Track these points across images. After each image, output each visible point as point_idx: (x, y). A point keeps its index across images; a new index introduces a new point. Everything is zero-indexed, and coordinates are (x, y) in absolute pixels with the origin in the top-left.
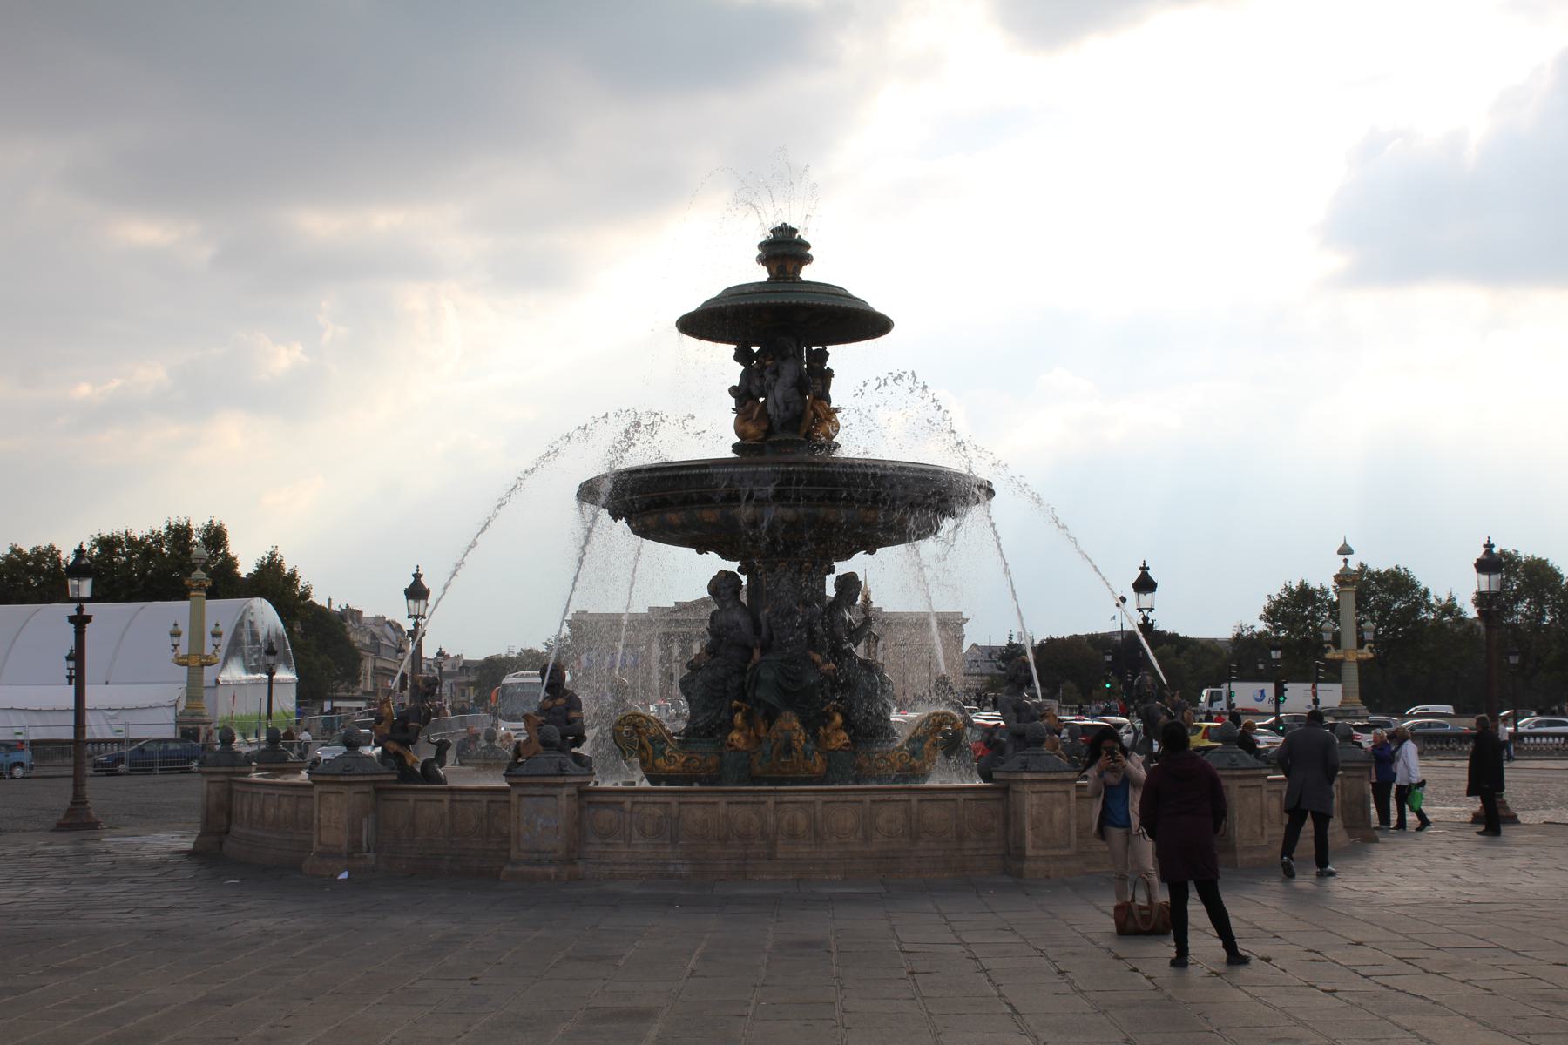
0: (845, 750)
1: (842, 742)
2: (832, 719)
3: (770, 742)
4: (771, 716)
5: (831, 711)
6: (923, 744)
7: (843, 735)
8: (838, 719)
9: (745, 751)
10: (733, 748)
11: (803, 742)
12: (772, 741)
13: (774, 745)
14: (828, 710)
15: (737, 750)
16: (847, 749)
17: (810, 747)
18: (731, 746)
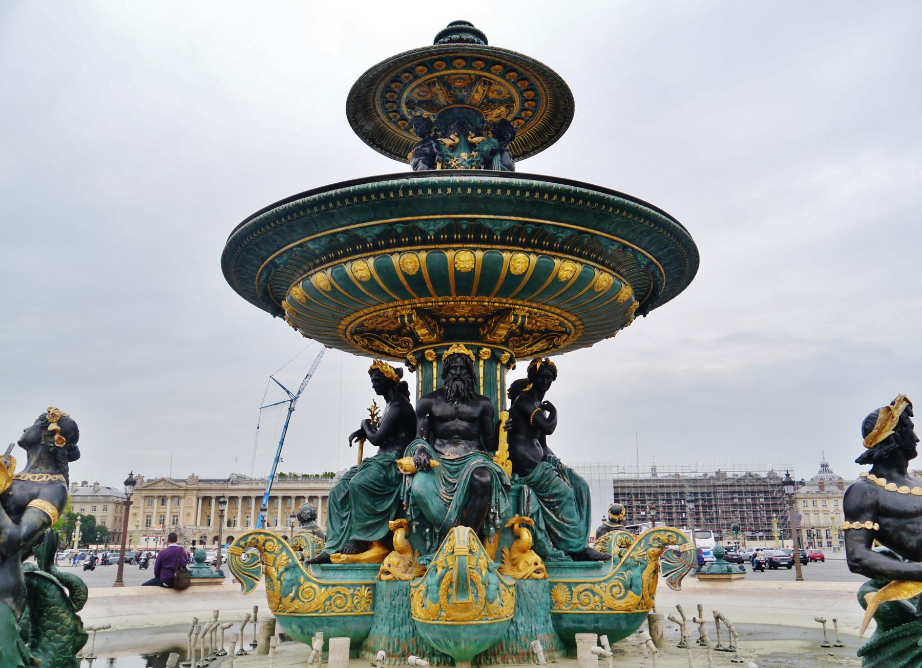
0: (537, 579)
1: (534, 568)
2: (518, 537)
3: (437, 570)
4: (441, 532)
5: (516, 526)
6: (642, 571)
7: (534, 557)
8: (526, 536)
9: (406, 580)
10: (390, 577)
11: (484, 572)
12: (440, 571)
13: (442, 577)
14: (513, 525)
15: (396, 580)
16: (540, 576)
17: (493, 579)
18: (388, 573)
